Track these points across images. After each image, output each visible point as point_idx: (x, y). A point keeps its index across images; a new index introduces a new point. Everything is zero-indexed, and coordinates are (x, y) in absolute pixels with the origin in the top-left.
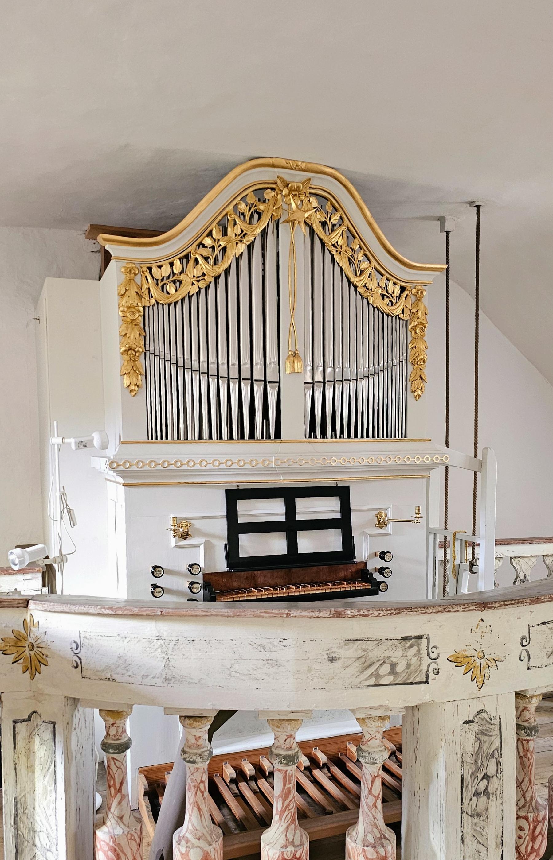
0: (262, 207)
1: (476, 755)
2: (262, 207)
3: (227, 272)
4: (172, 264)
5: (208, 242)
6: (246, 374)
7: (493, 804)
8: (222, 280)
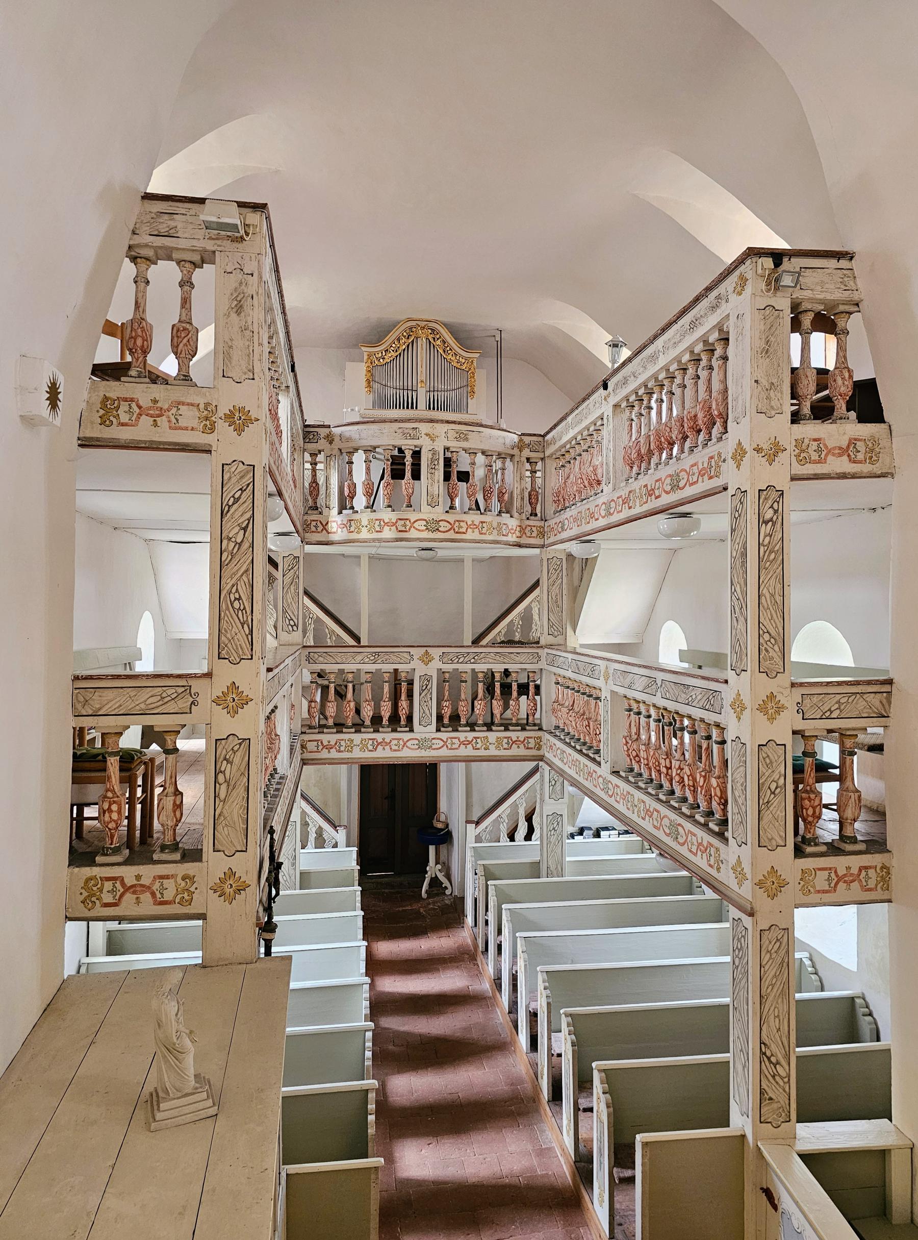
0: (411, 333)
1: (432, 459)
2: (411, 333)
3: (400, 354)
4: (382, 353)
5: (394, 345)
6: (406, 388)
7: (436, 472)
8: (398, 358)
